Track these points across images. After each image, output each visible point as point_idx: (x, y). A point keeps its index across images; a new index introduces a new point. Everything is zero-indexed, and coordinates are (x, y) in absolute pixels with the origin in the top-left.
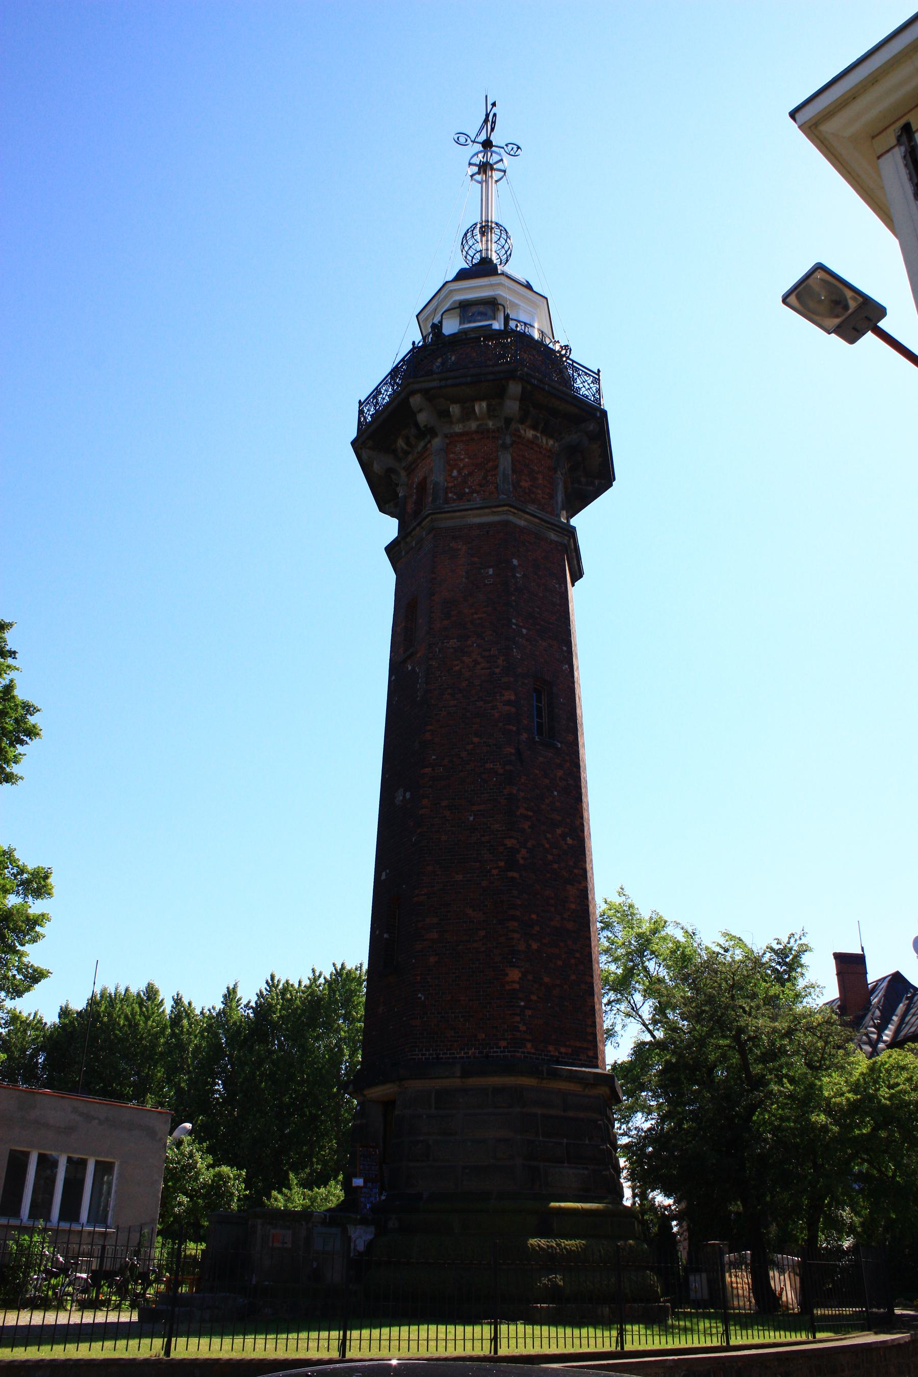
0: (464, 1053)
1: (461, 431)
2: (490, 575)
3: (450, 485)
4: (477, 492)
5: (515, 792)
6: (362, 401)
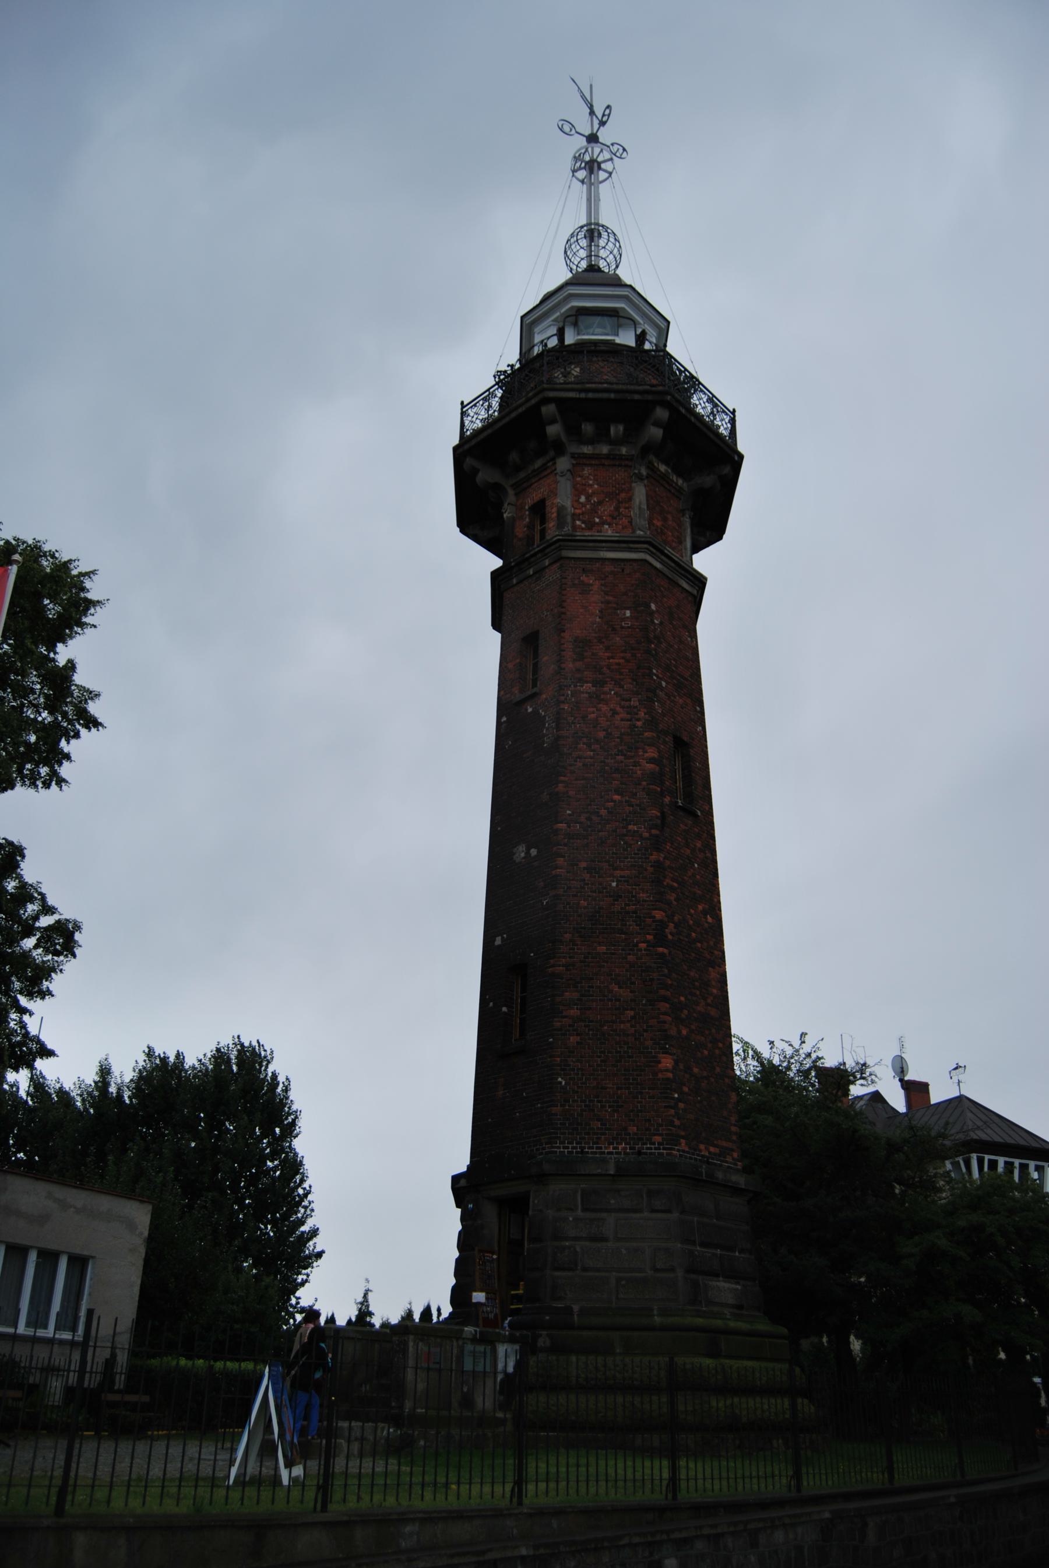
0: (614, 1148)
1: (591, 452)
2: (628, 618)
3: (578, 511)
4: (610, 525)
5: (661, 859)
6: (465, 403)
